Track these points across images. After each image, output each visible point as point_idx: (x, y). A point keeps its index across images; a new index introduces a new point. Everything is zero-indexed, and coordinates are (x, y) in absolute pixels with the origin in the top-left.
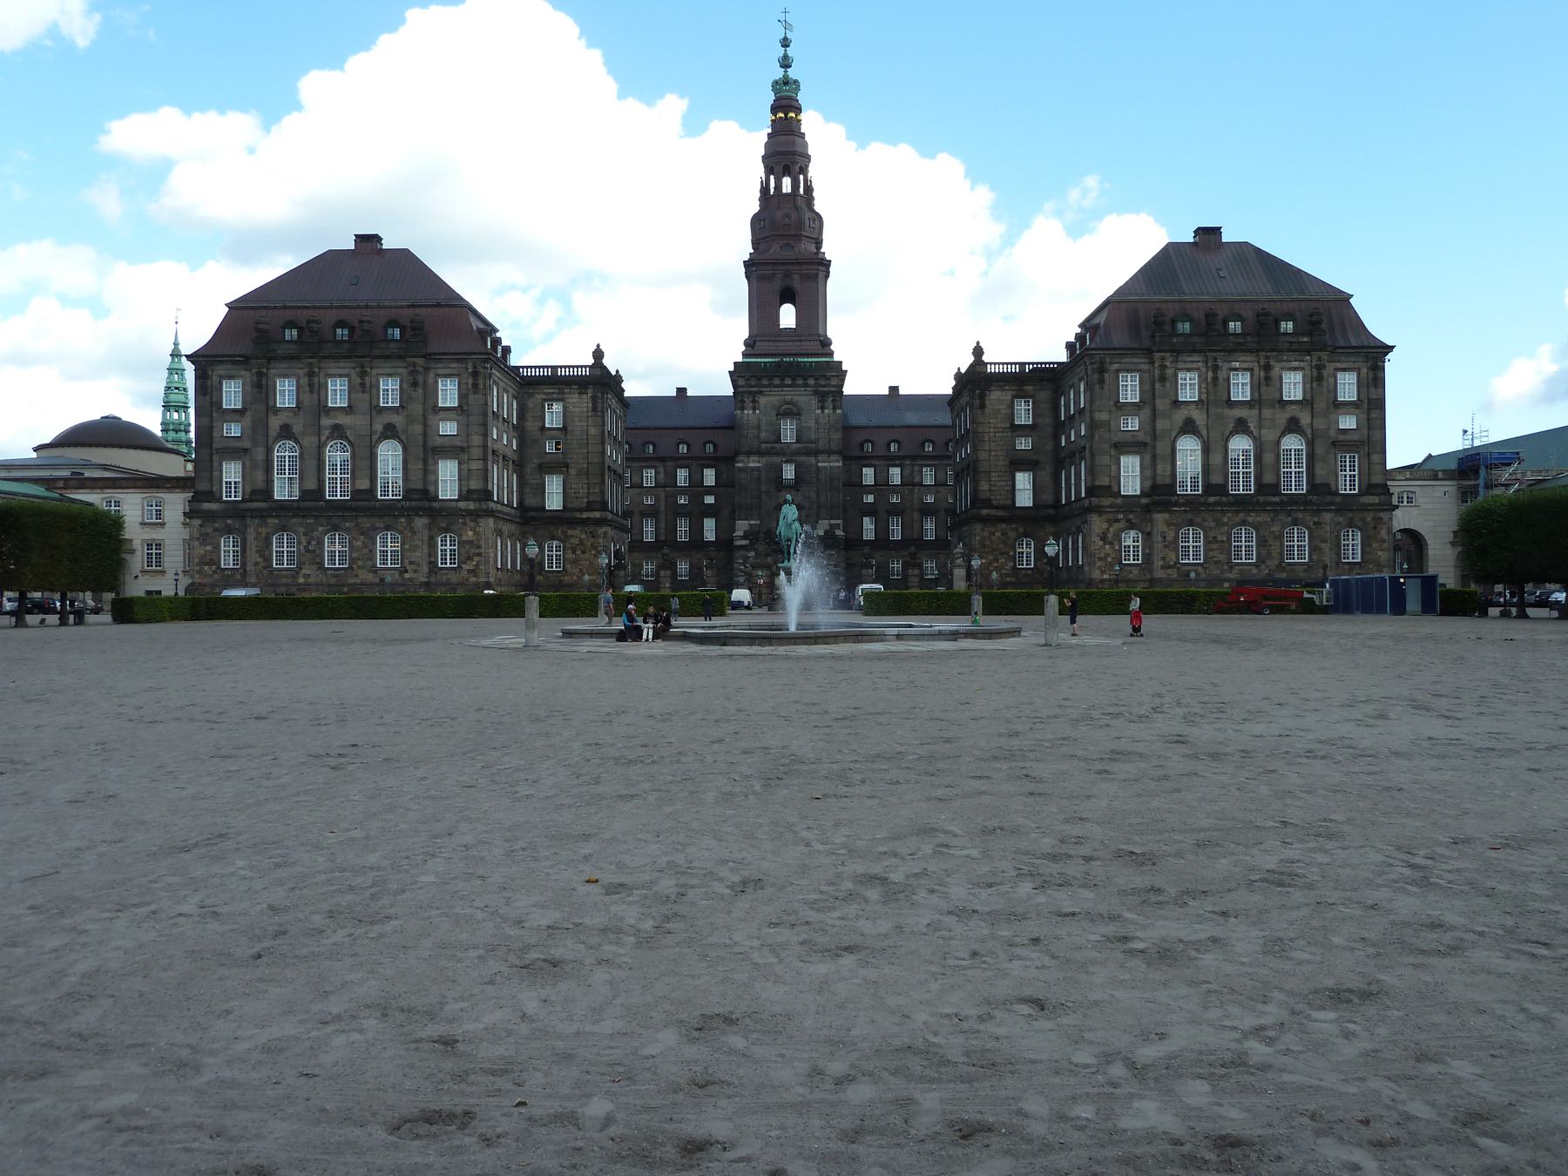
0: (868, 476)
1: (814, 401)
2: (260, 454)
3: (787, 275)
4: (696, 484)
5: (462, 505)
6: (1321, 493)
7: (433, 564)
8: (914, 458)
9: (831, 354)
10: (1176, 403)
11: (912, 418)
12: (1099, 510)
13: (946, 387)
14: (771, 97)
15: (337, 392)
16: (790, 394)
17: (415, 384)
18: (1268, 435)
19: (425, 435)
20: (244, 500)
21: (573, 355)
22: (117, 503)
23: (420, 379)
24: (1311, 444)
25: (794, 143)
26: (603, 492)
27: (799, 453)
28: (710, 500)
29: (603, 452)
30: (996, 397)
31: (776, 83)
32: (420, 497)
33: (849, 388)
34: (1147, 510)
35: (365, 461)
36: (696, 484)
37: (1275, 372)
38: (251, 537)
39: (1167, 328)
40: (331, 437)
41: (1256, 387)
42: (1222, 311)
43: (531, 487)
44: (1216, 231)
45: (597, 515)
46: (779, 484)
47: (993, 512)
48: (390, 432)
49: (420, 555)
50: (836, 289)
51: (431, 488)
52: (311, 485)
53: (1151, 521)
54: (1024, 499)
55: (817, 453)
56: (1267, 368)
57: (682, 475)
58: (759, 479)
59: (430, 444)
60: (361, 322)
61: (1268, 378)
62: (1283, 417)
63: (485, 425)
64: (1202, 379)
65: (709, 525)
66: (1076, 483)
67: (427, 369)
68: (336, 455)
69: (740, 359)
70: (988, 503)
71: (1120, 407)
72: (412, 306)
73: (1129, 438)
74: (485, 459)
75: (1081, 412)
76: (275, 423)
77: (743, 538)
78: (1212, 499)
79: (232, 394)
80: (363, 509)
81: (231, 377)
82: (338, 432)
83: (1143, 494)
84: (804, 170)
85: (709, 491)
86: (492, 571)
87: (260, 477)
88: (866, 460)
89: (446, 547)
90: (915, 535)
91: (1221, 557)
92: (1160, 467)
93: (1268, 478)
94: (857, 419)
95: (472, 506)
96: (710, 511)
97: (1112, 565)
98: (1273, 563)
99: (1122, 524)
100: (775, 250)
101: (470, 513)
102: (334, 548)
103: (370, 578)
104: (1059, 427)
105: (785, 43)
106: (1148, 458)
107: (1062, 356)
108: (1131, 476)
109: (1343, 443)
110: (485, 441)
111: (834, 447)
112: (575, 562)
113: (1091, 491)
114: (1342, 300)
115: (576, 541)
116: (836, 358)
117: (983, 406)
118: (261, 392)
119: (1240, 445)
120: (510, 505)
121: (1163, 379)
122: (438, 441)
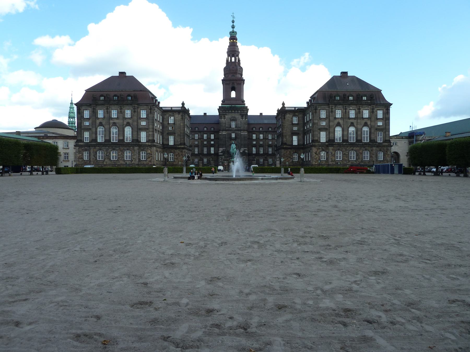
0: (254, 136)
1: (240, 117)
2: (94, 130)
3: (233, 83)
4: (209, 139)
5: (147, 143)
6: (373, 142)
7: (139, 159)
8: (266, 132)
9: (245, 104)
10: (335, 118)
11: (266, 122)
12: (315, 146)
13: (275, 113)
15: (114, 114)
16: (233, 115)
17: (135, 112)
18: (359, 127)
19: (137, 125)
20: (90, 142)
21: (177, 104)
22: (57, 143)
23: (136, 110)
24: (370, 129)
25: (235, 48)
26: (184, 140)
27: (236, 130)
28: (212, 143)
29: (184, 130)
30: (288, 116)
31: (230, 32)
32: (136, 142)
33: (249, 114)
34: (327, 146)
35: (121, 132)
36: (209, 139)
37: (361, 110)
38: (92, 152)
39: (333, 98)
40: (113, 126)
41: (356, 114)
42: (348, 94)
43: (166, 139)
44: (346, 73)
45: (183, 146)
46: (231, 139)
47: (287, 146)
48: (128, 124)
49: (136, 157)
51: (139, 139)
52: (108, 138)
53: (328, 149)
54: (295, 143)
55: (241, 130)
56: (359, 109)
57: (205, 136)
58: (225, 137)
59: (139, 127)
60: (120, 95)
61: (359, 112)
62: (363, 122)
63: (153, 122)
64: (342, 112)
65: (212, 149)
66: (309, 139)
67: (138, 108)
68: (114, 130)
69: (220, 105)
70: (286, 144)
71: (321, 119)
72: (134, 91)
73: (323, 127)
74: (153, 132)
75: (310, 120)
76: (98, 122)
77: (221, 153)
78: (344, 143)
79: (87, 114)
80: (121, 145)
81: (86, 110)
82: (115, 124)
83: (326, 142)
84: (238, 56)
85: (212, 140)
86: (155, 161)
87: (94, 136)
88: (254, 132)
89: (143, 155)
91: (347, 159)
92: (331, 135)
93: (359, 138)
94: (252, 122)
95: (150, 144)
96: (212, 146)
97: (318, 160)
98: (360, 160)
99: (321, 150)
101: (149, 146)
102: (114, 155)
103: (123, 163)
104: (305, 124)
105: (233, 22)
106: (328, 132)
107: (305, 105)
108: (323, 137)
109: (379, 129)
110: (153, 127)
111: (245, 129)
112: (177, 159)
113: (313, 141)
114: (379, 91)
115: (177, 153)
116: (246, 105)
117: (285, 118)
118: (94, 114)
119: (352, 129)
120: (160, 144)
121: (332, 112)
122: (141, 127)
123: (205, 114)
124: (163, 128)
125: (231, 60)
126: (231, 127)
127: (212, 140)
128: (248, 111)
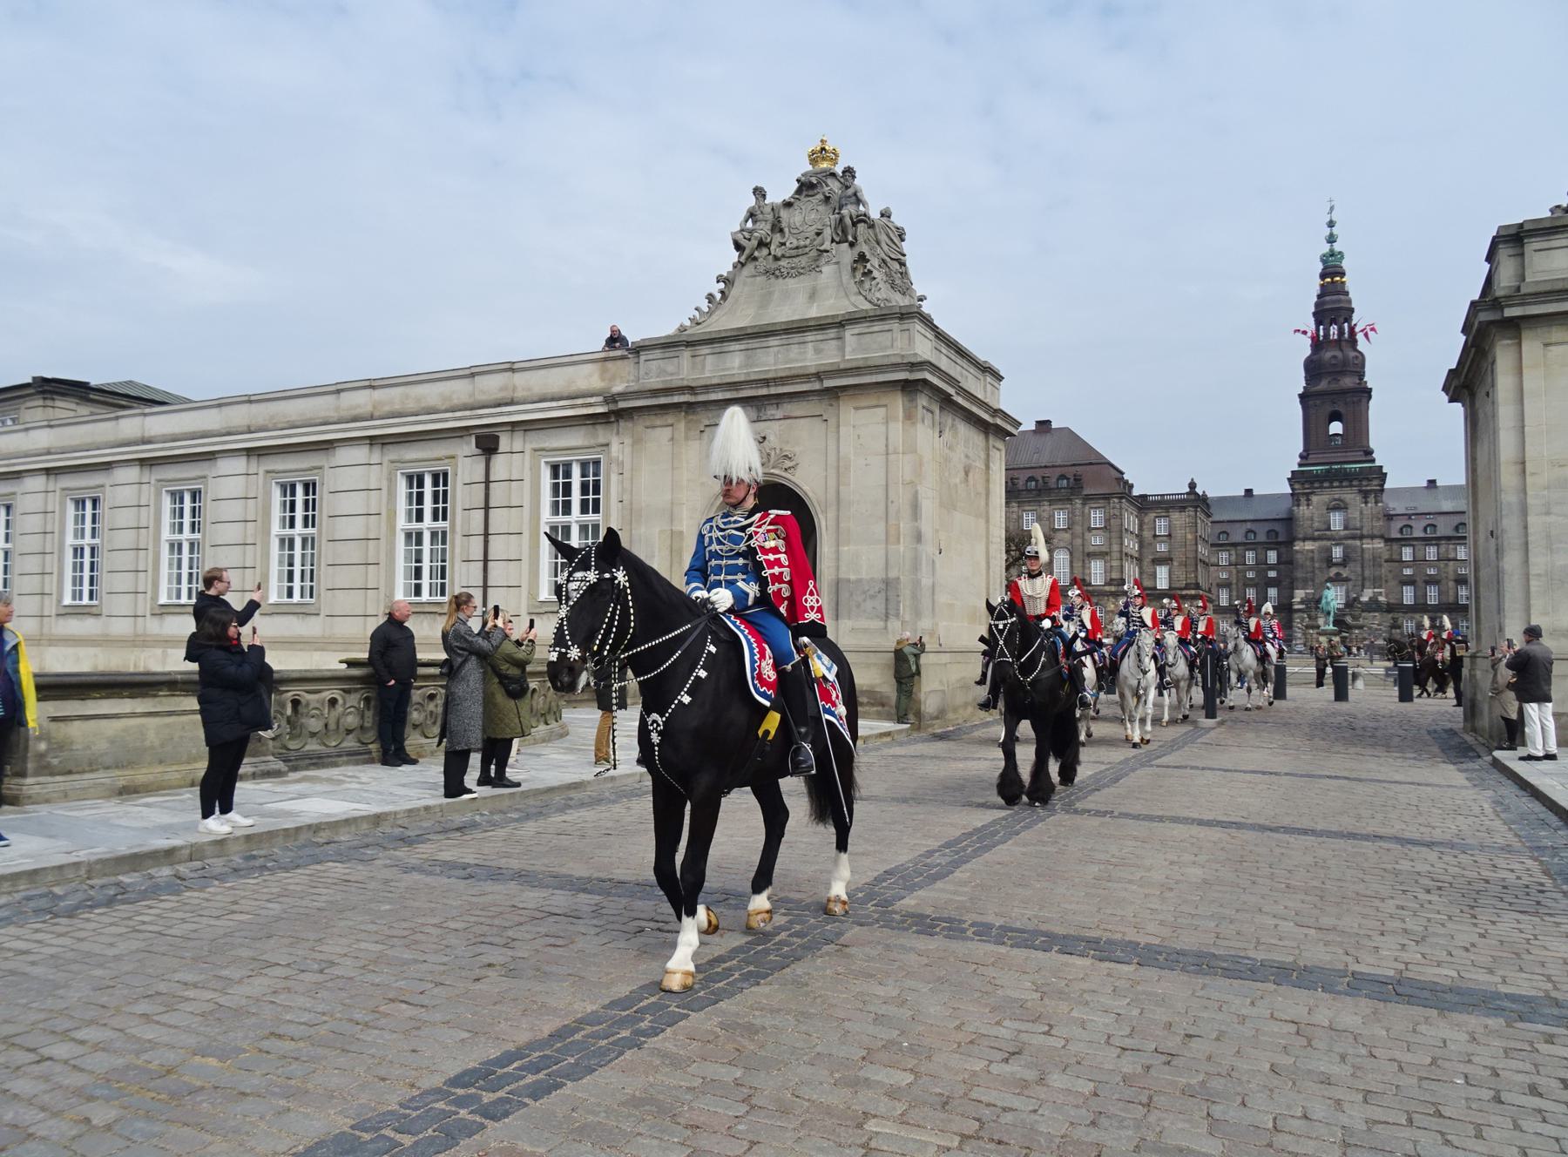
1: (1359, 498)
4: (1262, 564)
5: (1107, 588)
8: (1449, 538)
9: (1373, 461)
14: (1320, 267)
16: (1337, 493)
27: (1347, 538)
28: (1272, 574)
43: (1147, 574)
46: (1329, 562)
50: (1376, 410)
55: (1361, 537)
58: (1312, 559)
69: (1296, 468)
84: (1348, 319)
85: (1272, 567)
90: (1451, 599)
95: (1113, 589)
100: (1323, 385)
105: (1331, 224)
122: (1092, 549)
123: (1249, 492)
124: (1141, 546)
125: (1327, 335)
126: (1329, 529)
127: (1272, 567)
128: (1384, 480)
